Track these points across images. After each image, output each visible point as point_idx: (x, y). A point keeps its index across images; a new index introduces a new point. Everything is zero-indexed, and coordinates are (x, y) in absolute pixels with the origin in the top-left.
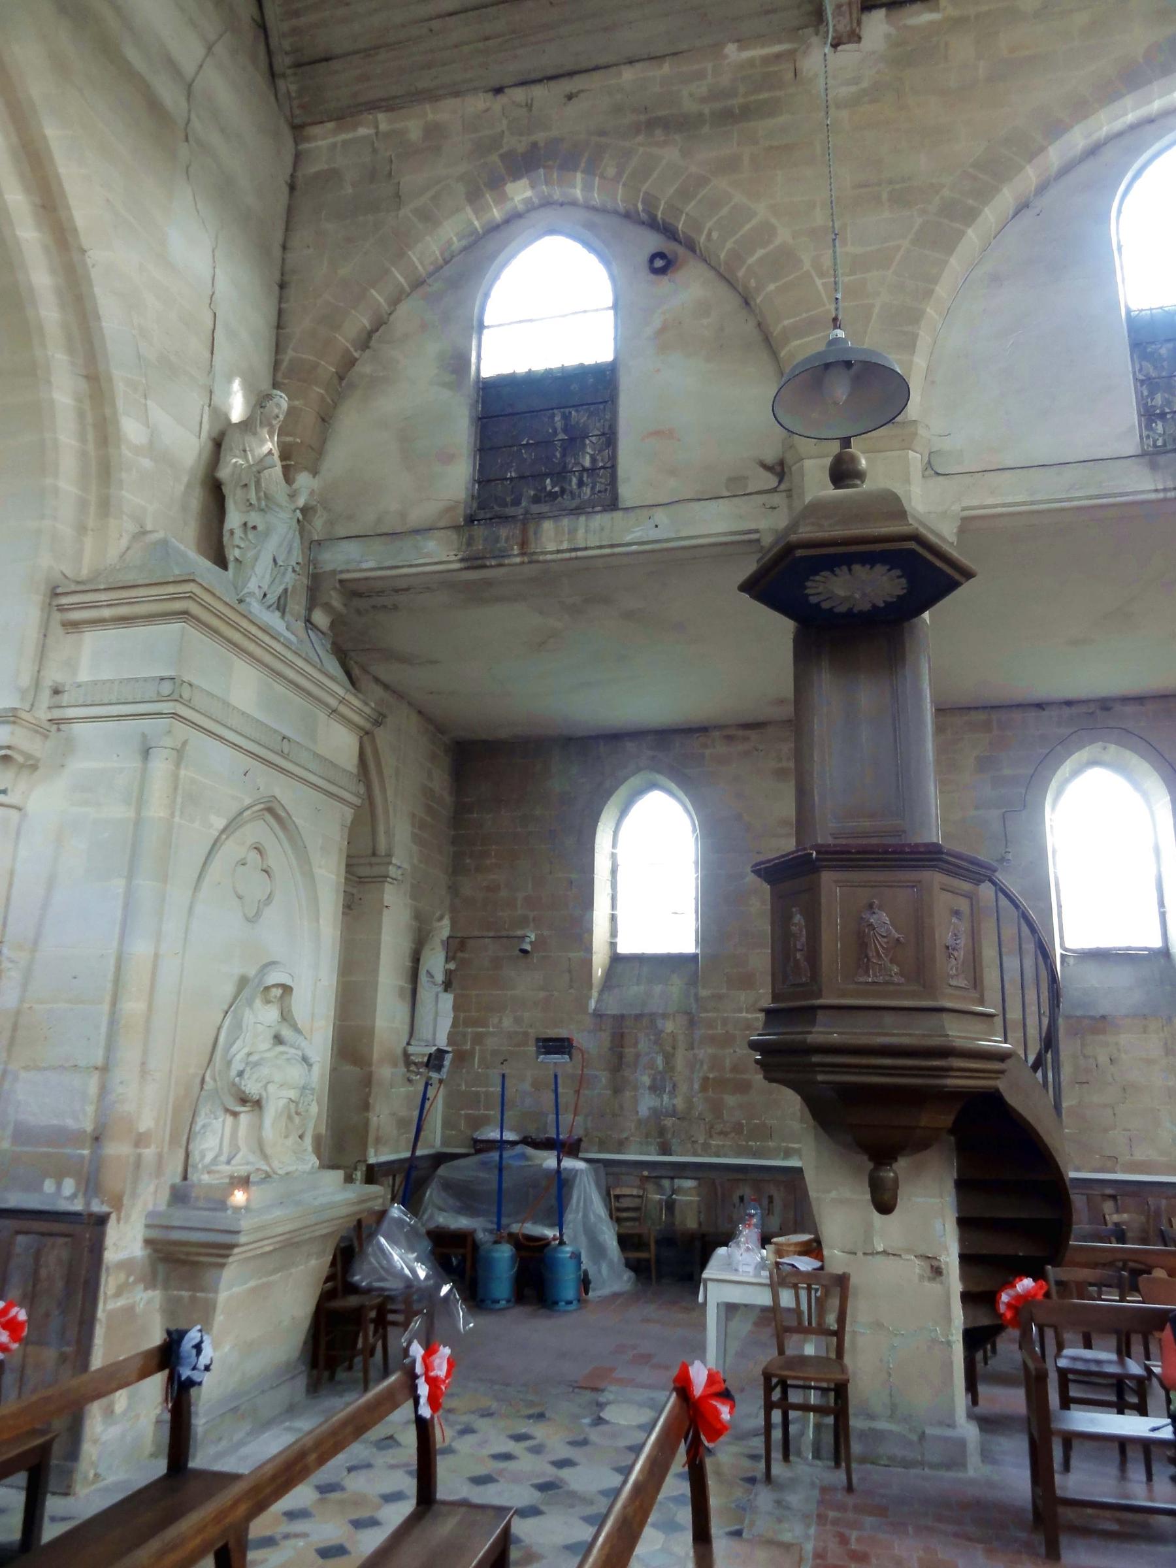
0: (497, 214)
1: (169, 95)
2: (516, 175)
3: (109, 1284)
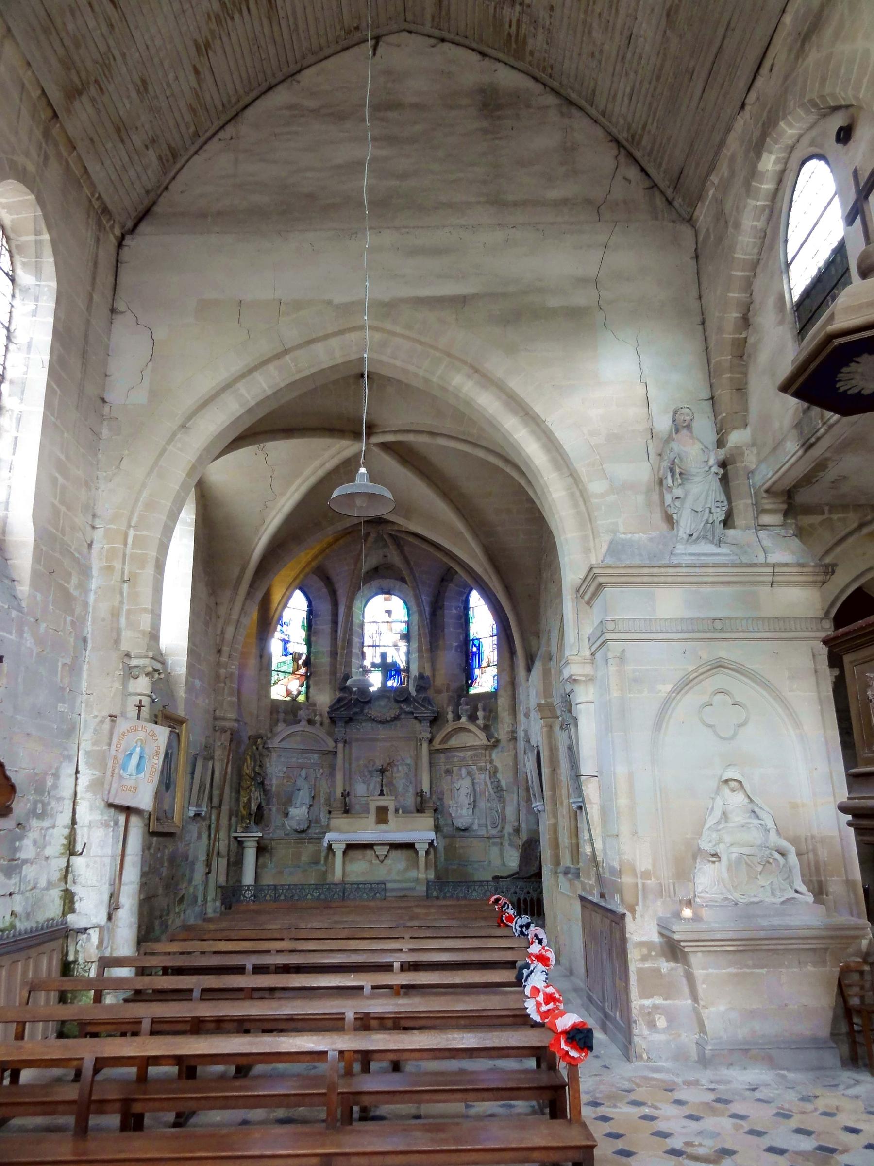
0: (767, 186)
1: (581, 298)
2: (759, 156)
3: (634, 955)
